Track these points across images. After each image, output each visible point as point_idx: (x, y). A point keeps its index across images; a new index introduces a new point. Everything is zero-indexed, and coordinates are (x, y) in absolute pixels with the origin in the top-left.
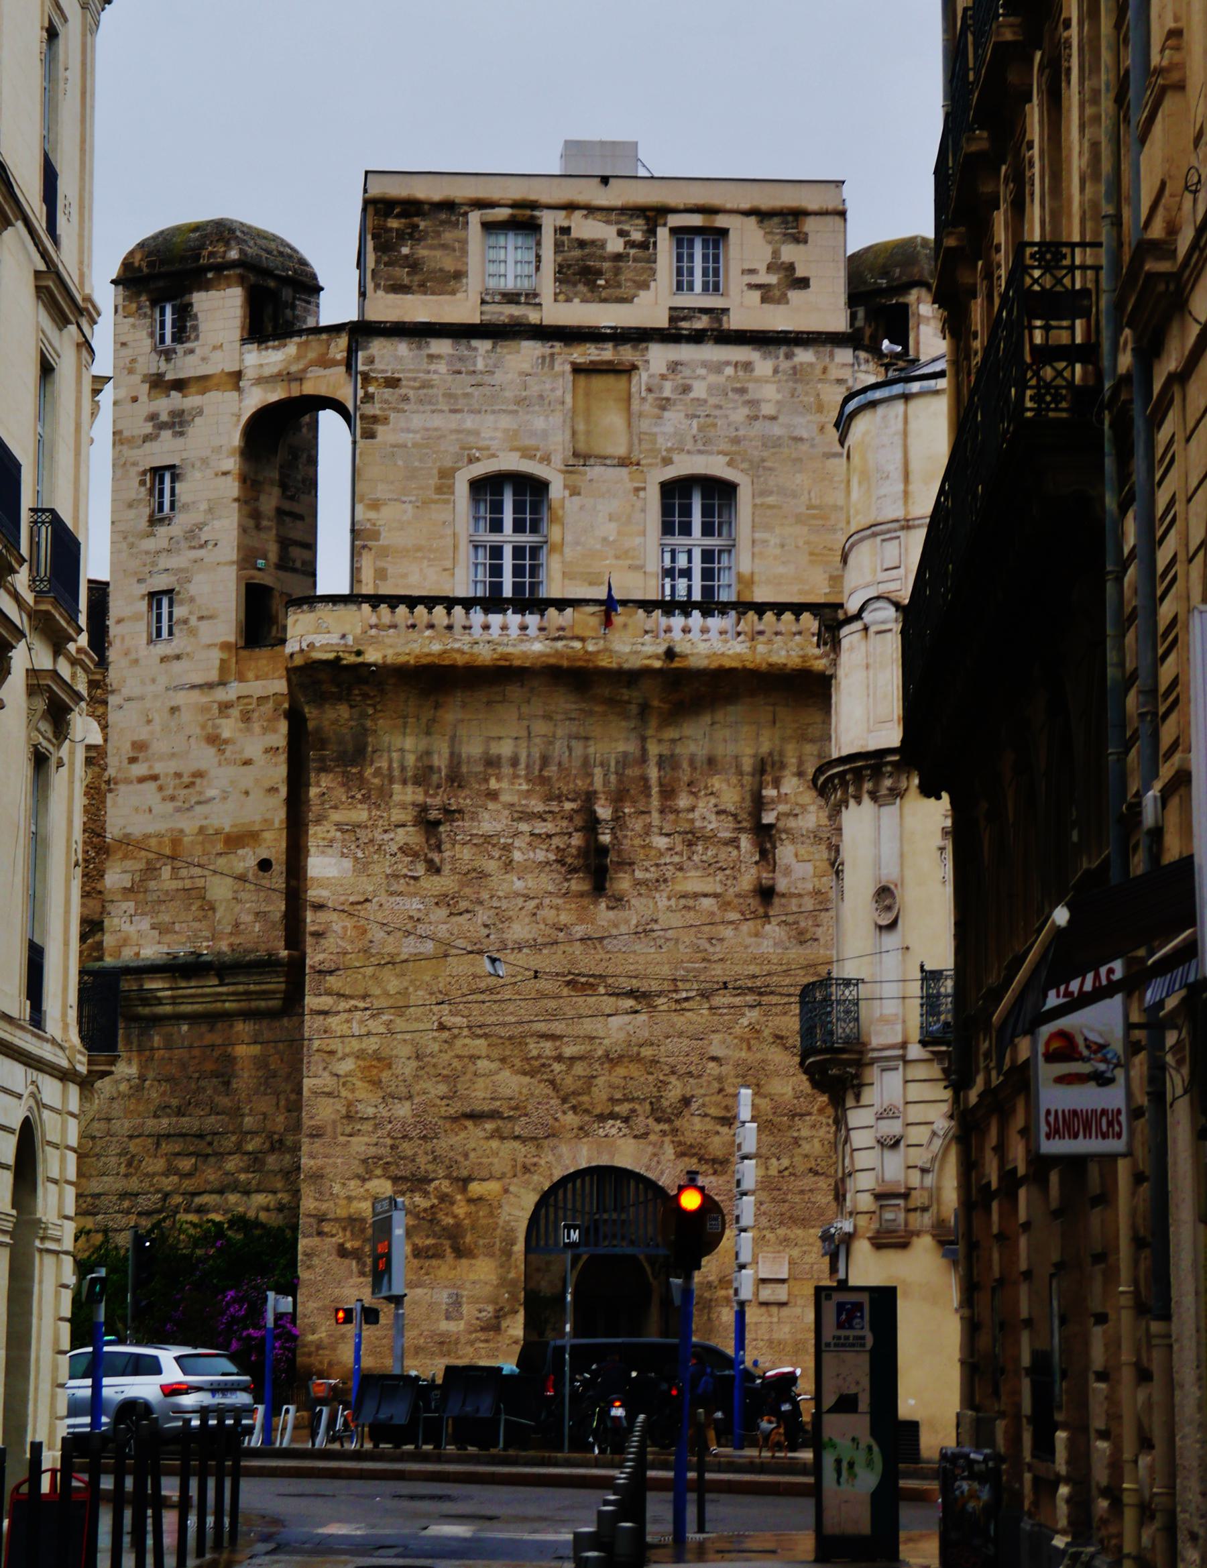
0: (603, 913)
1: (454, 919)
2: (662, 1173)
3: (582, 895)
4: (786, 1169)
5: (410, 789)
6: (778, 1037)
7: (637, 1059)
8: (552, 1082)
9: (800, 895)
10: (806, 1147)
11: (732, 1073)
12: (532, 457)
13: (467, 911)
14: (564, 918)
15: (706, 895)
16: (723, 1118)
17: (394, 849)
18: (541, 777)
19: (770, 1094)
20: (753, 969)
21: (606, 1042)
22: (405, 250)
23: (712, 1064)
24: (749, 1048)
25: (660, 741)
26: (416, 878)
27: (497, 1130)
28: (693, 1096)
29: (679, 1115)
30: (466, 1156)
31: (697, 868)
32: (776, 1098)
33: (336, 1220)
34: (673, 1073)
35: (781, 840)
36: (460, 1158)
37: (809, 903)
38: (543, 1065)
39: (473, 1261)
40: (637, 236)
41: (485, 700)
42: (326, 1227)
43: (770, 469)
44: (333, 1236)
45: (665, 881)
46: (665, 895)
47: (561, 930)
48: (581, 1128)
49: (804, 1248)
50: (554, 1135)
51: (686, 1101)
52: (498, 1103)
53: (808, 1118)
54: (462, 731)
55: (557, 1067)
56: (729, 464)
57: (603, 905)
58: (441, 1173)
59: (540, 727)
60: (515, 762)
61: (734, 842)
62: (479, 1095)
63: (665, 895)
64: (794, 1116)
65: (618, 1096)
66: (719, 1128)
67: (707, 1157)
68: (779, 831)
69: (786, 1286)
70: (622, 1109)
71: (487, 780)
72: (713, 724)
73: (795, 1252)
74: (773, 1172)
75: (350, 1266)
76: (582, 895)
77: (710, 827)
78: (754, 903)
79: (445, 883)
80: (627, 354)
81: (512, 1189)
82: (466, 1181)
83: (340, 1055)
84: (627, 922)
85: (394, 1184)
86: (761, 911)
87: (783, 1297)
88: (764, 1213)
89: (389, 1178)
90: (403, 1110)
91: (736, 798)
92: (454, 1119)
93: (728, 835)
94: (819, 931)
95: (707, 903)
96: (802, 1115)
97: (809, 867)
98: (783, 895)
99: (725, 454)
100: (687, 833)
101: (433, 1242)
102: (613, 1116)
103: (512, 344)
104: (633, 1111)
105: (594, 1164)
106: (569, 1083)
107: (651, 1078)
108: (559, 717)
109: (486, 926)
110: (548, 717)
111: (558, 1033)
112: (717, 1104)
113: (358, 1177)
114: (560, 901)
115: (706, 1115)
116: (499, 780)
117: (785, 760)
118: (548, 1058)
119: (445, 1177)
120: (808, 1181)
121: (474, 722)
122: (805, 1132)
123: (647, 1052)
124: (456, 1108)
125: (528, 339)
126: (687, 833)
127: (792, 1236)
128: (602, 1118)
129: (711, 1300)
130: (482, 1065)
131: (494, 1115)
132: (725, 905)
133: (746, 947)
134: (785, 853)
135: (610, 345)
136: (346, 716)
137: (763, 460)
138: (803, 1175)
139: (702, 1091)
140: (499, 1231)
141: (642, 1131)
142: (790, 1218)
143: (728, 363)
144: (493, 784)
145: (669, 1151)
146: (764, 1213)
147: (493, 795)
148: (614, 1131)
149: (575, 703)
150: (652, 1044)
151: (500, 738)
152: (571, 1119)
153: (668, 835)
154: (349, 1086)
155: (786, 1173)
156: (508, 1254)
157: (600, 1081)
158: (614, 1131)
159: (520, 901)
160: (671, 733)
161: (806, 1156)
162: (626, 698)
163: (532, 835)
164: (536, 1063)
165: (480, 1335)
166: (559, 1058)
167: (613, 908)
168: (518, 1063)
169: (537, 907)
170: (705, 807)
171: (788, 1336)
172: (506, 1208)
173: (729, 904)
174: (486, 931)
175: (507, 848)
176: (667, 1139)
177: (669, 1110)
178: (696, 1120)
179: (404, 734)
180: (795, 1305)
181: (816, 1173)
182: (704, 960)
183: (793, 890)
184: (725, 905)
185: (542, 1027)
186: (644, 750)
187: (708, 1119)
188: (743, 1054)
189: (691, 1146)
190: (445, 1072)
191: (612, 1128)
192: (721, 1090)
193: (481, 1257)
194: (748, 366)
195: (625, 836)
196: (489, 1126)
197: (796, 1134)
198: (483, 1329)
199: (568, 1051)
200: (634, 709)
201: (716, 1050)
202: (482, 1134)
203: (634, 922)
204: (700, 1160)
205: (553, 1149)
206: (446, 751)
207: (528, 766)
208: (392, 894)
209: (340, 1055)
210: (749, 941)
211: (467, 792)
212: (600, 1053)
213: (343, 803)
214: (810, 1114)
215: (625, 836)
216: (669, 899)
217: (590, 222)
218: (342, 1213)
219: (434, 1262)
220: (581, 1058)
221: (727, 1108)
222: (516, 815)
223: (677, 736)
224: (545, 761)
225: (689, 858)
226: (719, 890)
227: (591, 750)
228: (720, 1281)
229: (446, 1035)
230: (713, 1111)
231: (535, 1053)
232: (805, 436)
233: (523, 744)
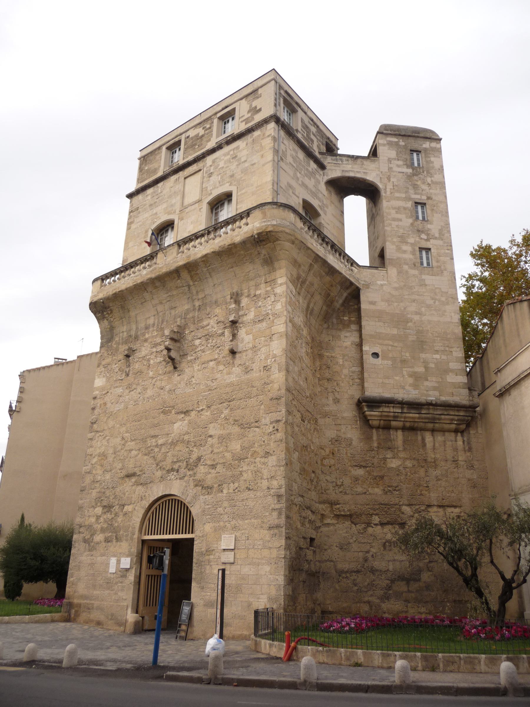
0: (176, 378)
1: (131, 393)
2: (188, 496)
3: (170, 372)
4: (237, 488)
5: (124, 345)
6: (235, 421)
7: (183, 441)
8: (154, 457)
9: (247, 350)
10: (245, 475)
11: (217, 442)
12: (171, 214)
13: (135, 389)
14: (163, 384)
15: (211, 361)
16: (212, 465)
17: (117, 370)
18: (161, 328)
19: (231, 450)
20: (228, 390)
21: (173, 435)
22: (146, 168)
23: (209, 439)
24: (224, 429)
25: (198, 299)
26: (122, 380)
27: (136, 482)
28: (202, 456)
29: (196, 466)
30: (125, 494)
31: (209, 349)
32: (233, 451)
33: (85, 526)
34: (195, 446)
35: (241, 327)
36: (122, 496)
37: (250, 353)
38: (152, 450)
39: (121, 543)
40: (208, 126)
41: (140, 303)
42: (82, 530)
43: (244, 180)
44: (83, 533)
45: (198, 358)
46: (197, 364)
47: (162, 389)
48: (162, 477)
49: (243, 532)
50: (152, 482)
51: (199, 459)
52: (136, 469)
53: (246, 460)
54: (139, 319)
55: (156, 450)
56: (230, 185)
57: (176, 375)
58: (117, 502)
59: (160, 308)
60: (154, 325)
61: (223, 334)
62: (130, 466)
63: (197, 364)
64: (241, 459)
65: (175, 460)
66: (211, 471)
67: (205, 486)
68: (240, 324)
69: (233, 553)
70: (176, 467)
71: (145, 335)
72: (214, 285)
73: (238, 534)
74: (231, 491)
75: (86, 546)
76: (170, 372)
77: (214, 330)
78: (229, 358)
79: (131, 378)
80: (200, 165)
81: (136, 508)
82: (124, 506)
83: (93, 456)
84: (184, 380)
85: (103, 509)
86: (231, 361)
87: (232, 560)
88: (226, 513)
89: (102, 506)
90: (108, 476)
91: (224, 314)
92: (123, 478)
93: (221, 331)
94: (254, 365)
95: (212, 364)
96: (244, 459)
97: (251, 336)
98: (240, 352)
99: (228, 182)
100: (206, 335)
101: (110, 534)
102: (172, 470)
103: (168, 180)
104: (180, 466)
105: (164, 494)
106: (159, 457)
107: (187, 449)
108: (164, 301)
109: (139, 393)
110: (161, 303)
111: (157, 434)
112: (210, 459)
113: (93, 507)
114: (162, 377)
115: (206, 465)
116: (148, 334)
117: (243, 292)
118: (153, 446)
119: (117, 505)
120: (246, 494)
121: (141, 314)
122: (245, 468)
123: (186, 437)
124: (124, 473)
125: (172, 175)
126: (206, 335)
127: (238, 525)
128: (168, 471)
129: (202, 561)
130: (134, 453)
131: (134, 475)
132: (218, 363)
133: (225, 380)
134: (242, 333)
135: (195, 165)
136: (107, 324)
137: (241, 178)
138: (244, 491)
139: (205, 453)
140: (130, 528)
141: (182, 476)
142: (237, 515)
143: (231, 150)
144: (147, 336)
145: (192, 484)
146: (226, 513)
147: (146, 340)
148: (173, 477)
149: (167, 293)
150: (188, 433)
151: (149, 317)
152: (159, 473)
153: (200, 338)
154: (95, 468)
155: (236, 491)
156: (132, 539)
157: (169, 454)
158: (173, 477)
159: (150, 380)
160: (201, 296)
161: (245, 480)
162: (181, 284)
163: (157, 352)
164: (149, 449)
165: (120, 579)
166: (157, 446)
167: (180, 375)
168: (143, 449)
169: (156, 382)
170: (212, 322)
171: (234, 582)
172: (133, 518)
173: (219, 362)
174: (140, 396)
175: (149, 360)
176: (191, 479)
177: (192, 464)
178: (202, 467)
179: (123, 325)
180: (238, 564)
181: (249, 489)
182: (210, 390)
183: (244, 349)
184: (218, 363)
185: (152, 433)
186: (194, 306)
187: (206, 467)
188: (221, 432)
189: (200, 481)
190: (122, 458)
191: (172, 476)
192: (212, 451)
193: (124, 541)
194: (238, 148)
195: (185, 343)
196: (133, 480)
197: (241, 470)
198: (121, 576)
199: (160, 442)
200: (186, 288)
201: (211, 432)
202: (131, 484)
203: (186, 379)
204: (203, 487)
205: (151, 488)
206: (134, 327)
207: (158, 325)
208: (114, 388)
209: (93, 456)
210: (226, 377)
211: (139, 341)
212: (170, 441)
213: (106, 357)
214: (247, 458)
215: (185, 343)
216: (198, 366)
217: (196, 130)
218: (87, 523)
219: (109, 544)
220: (164, 444)
221: (214, 460)
222: (152, 346)
223: (204, 296)
224: (162, 322)
225: (207, 346)
226: (216, 357)
227: (177, 312)
228: (206, 551)
229: (123, 442)
230: (209, 463)
231: (149, 445)
232: (256, 161)
233: (156, 317)
